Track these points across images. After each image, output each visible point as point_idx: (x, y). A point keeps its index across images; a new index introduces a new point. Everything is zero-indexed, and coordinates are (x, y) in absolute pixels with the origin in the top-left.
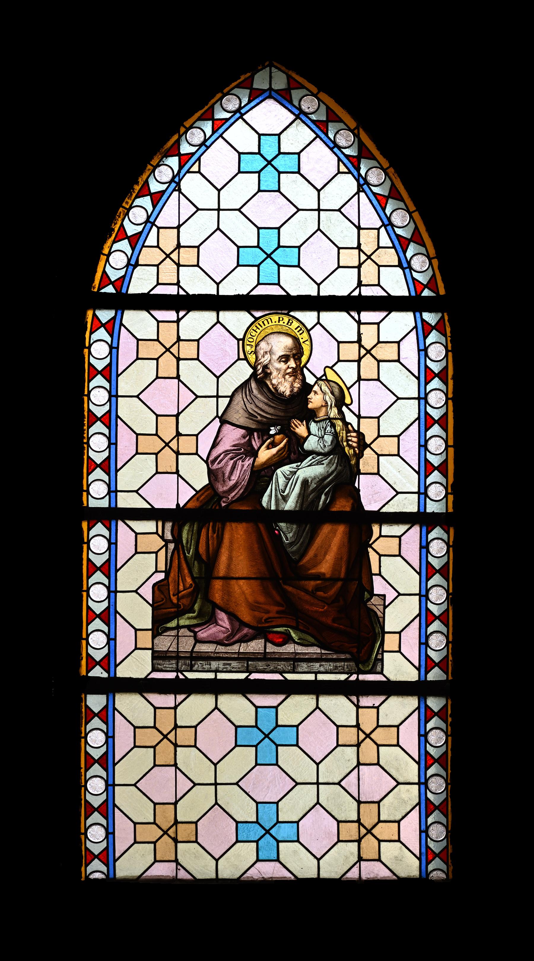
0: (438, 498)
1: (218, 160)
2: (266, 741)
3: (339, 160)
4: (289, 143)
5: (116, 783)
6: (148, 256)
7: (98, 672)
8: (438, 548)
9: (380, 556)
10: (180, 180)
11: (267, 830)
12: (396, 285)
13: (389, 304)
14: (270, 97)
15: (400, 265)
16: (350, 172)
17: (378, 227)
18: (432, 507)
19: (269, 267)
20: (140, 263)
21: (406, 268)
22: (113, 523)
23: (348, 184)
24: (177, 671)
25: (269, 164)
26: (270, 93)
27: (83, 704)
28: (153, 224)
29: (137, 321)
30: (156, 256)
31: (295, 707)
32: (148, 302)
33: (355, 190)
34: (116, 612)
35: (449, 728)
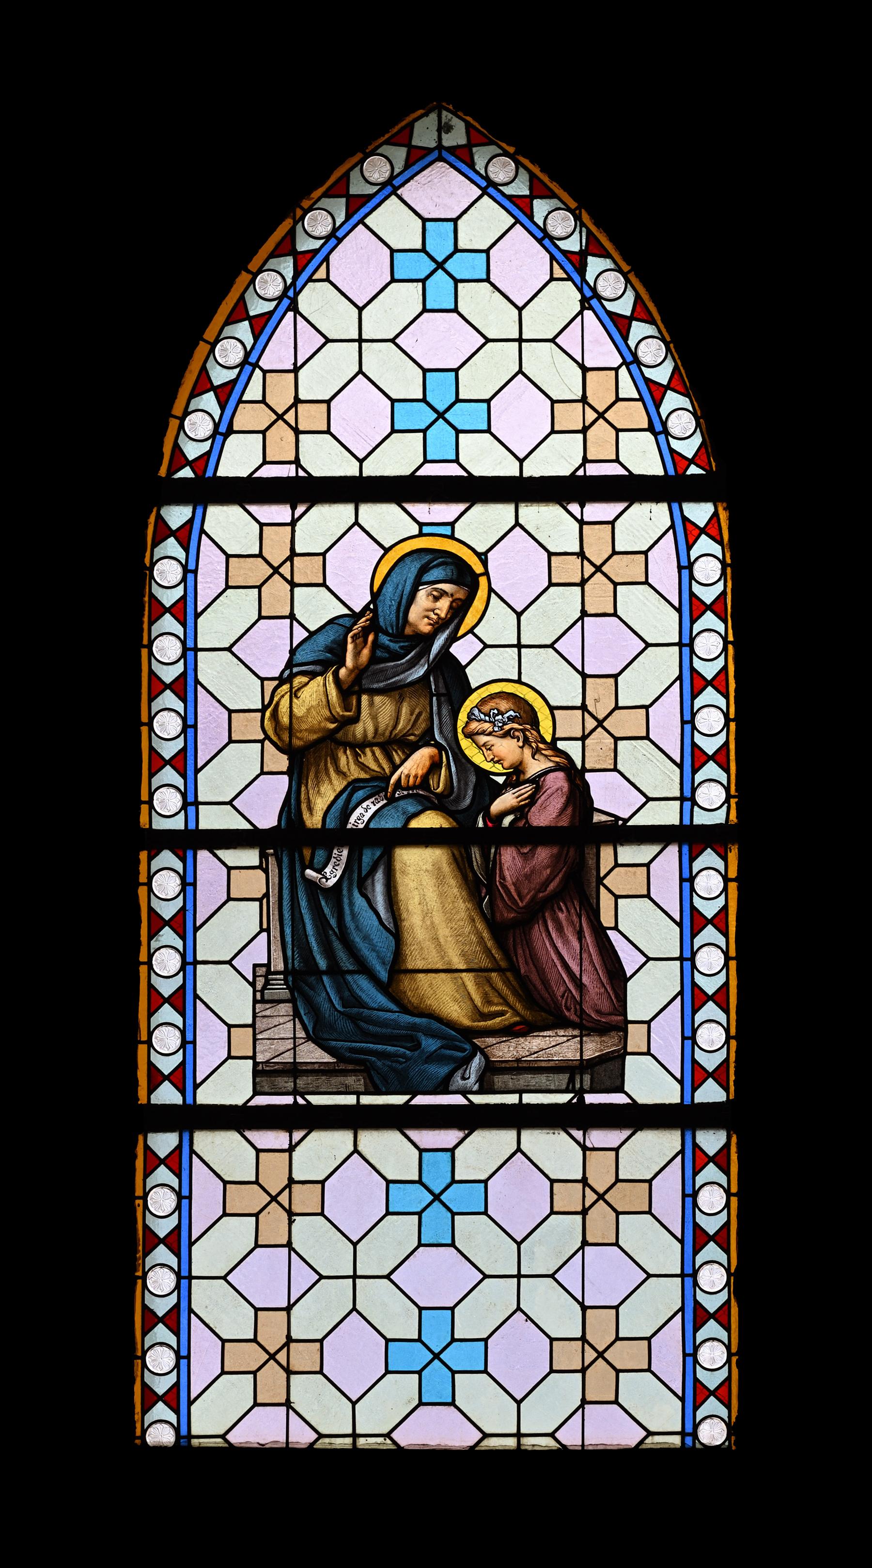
0: (713, 801)
1: (357, 261)
2: (437, 1203)
3: (552, 258)
4: (472, 234)
5: (194, 1274)
6: (246, 417)
7: (167, 1095)
8: (709, 883)
9: (617, 897)
10: (297, 294)
11: (437, 1203)
12: (643, 458)
13: (630, 489)
14: (441, 159)
15: (651, 429)
16: (569, 278)
17: (616, 366)
18: (701, 818)
19: (441, 433)
20: (235, 428)
21: (660, 433)
22: (189, 854)
23: (567, 296)
24: (295, 1093)
25: (439, 268)
26: (440, 153)
27: (147, 590)
28: (256, 365)
29: (227, 523)
30: (259, 417)
31: (483, 1149)
32: (247, 491)
33: (578, 308)
34: (197, 682)
35: (730, 631)
